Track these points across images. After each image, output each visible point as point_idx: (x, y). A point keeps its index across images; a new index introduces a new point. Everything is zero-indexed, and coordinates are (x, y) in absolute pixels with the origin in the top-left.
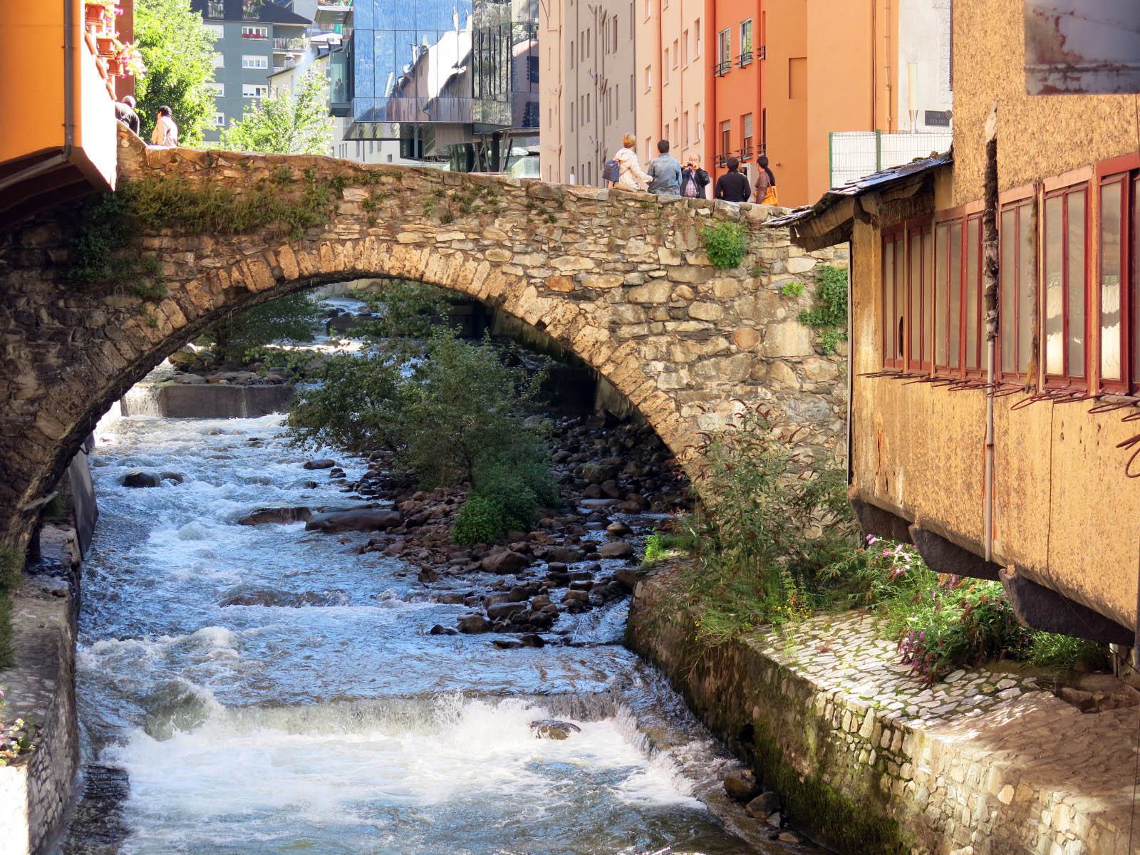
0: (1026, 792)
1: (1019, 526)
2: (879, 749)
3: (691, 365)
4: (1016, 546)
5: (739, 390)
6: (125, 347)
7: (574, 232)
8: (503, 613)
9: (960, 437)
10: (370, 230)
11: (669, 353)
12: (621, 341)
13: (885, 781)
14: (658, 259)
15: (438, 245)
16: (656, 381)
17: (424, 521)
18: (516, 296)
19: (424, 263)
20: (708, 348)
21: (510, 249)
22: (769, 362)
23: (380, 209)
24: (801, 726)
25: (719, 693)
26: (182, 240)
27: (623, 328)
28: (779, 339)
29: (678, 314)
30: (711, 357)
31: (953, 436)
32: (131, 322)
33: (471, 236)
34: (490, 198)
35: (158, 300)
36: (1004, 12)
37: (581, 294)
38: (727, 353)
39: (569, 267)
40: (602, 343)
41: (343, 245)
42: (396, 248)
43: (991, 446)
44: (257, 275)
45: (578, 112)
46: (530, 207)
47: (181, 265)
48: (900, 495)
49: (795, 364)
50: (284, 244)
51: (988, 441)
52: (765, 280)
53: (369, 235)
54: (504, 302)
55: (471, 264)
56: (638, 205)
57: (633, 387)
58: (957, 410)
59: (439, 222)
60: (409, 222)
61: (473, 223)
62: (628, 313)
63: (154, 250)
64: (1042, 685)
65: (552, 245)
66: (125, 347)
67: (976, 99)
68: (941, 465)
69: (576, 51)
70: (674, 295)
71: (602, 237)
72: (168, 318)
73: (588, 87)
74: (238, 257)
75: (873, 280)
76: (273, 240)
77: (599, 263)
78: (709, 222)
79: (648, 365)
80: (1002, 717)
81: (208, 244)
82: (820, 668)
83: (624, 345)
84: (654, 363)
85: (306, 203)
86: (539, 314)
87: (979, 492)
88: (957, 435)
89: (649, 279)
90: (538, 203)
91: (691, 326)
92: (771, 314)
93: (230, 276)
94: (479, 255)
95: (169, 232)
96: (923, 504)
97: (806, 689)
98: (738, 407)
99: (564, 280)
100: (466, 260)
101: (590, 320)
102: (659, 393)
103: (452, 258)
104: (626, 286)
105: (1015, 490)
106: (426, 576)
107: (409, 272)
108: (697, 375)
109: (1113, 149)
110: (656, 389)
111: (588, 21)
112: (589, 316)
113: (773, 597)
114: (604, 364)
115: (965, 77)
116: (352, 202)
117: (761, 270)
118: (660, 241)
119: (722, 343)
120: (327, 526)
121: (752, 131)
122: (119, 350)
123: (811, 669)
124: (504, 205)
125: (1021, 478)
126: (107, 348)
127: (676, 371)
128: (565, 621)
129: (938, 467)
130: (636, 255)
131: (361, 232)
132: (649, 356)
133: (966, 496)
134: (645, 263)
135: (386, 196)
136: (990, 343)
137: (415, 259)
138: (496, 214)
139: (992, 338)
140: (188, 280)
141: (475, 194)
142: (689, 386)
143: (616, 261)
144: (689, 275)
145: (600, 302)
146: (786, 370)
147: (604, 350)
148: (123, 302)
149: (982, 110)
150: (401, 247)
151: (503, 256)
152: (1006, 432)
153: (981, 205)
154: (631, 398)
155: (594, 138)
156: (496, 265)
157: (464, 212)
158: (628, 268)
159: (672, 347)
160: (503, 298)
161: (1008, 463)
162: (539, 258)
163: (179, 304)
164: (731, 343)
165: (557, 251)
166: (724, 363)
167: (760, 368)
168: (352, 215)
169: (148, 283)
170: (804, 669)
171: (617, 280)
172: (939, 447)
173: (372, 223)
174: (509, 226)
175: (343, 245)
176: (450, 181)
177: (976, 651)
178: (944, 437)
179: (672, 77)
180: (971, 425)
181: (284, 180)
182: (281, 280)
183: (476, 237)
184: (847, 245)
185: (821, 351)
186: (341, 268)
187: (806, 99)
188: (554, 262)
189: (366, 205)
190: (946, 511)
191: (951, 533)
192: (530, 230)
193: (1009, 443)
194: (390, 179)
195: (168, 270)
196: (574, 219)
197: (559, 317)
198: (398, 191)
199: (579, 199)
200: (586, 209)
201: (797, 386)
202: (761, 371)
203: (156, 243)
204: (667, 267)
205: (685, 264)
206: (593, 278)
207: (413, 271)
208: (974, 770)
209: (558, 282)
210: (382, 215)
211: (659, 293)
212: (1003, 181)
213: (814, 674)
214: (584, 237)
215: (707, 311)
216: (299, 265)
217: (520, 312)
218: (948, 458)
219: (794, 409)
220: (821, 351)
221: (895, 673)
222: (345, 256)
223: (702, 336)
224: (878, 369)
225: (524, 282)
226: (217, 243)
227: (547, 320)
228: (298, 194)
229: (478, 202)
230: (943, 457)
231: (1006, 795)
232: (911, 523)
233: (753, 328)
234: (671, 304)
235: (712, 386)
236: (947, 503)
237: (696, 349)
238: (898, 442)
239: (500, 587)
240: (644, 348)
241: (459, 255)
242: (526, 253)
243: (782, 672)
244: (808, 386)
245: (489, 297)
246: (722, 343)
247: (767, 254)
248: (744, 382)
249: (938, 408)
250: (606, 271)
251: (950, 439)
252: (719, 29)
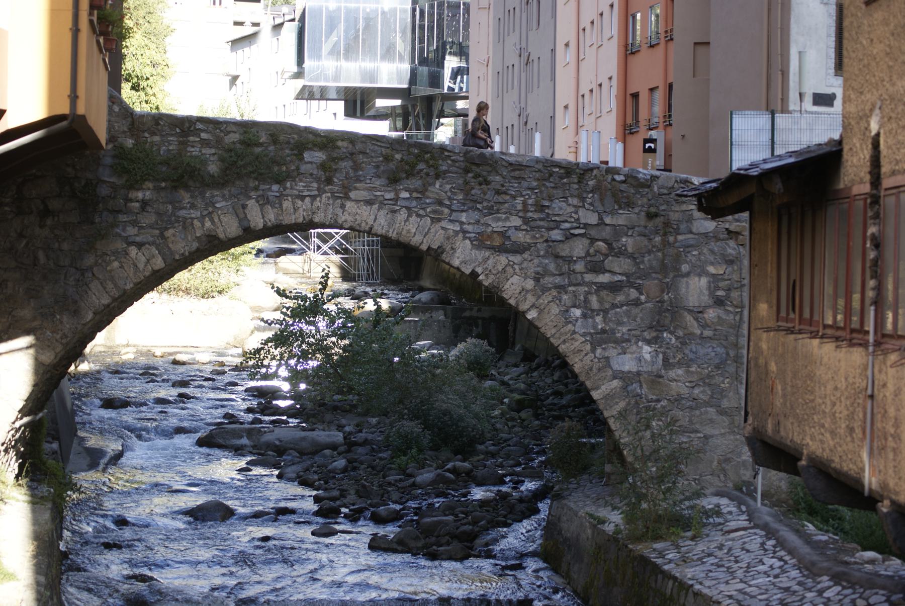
1: (895, 467)
3: (605, 312)
4: (891, 484)
5: (647, 335)
6: (110, 285)
7: (505, 193)
9: (844, 387)
10: (327, 188)
11: (586, 301)
12: (545, 290)
14: (578, 219)
15: (386, 202)
16: (574, 325)
18: (452, 248)
19: (373, 217)
20: (620, 298)
21: (449, 207)
23: (336, 170)
26: (163, 194)
27: (546, 278)
28: (683, 291)
29: (596, 268)
30: (622, 305)
31: (839, 386)
32: (116, 264)
33: (415, 195)
34: (431, 162)
36: (887, 25)
38: (637, 303)
39: (500, 224)
40: (527, 291)
41: (303, 200)
42: (349, 204)
43: (872, 397)
46: (467, 171)
49: (697, 313)
50: (250, 198)
51: (869, 392)
52: (671, 239)
53: (325, 192)
54: (442, 253)
55: (414, 219)
56: (562, 171)
57: (553, 331)
58: (843, 364)
59: (387, 181)
60: (361, 181)
61: (416, 183)
63: (138, 201)
65: (485, 204)
66: (110, 285)
67: (863, 97)
68: (827, 411)
70: (592, 251)
71: (530, 198)
72: (148, 260)
73: (512, 58)
74: (210, 209)
75: (770, 246)
77: (526, 221)
78: (623, 187)
79: (567, 311)
82: (714, 582)
83: (547, 294)
84: (573, 310)
86: (473, 265)
87: (860, 435)
88: (842, 384)
89: (569, 237)
90: (474, 167)
91: (604, 278)
92: (678, 270)
93: (203, 225)
94: (421, 212)
95: (150, 185)
96: (811, 443)
98: (647, 351)
99: (495, 235)
100: (410, 216)
101: (517, 270)
102: (577, 336)
103: (397, 215)
105: (892, 435)
107: (360, 225)
108: (610, 320)
110: (574, 332)
112: (516, 267)
114: (529, 310)
115: (854, 77)
116: (311, 163)
122: (105, 288)
123: (708, 583)
124: (444, 168)
125: (897, 425)
127: (591, 317)
129: (824, 412)
130: (558, 215)
131: (318, 189)
132: (569, 303)
133: (849, 439)
134: (566, 221)
135: (342, 159)
136: (872, 308)
137: (365, 214)
138: (437, 176)
140: (167, 229)
142: (603, 331)
143: (541, 219)
145: (526, 255)
146: (689, 318)
147: (529, 296)
149: (868, 107)
150: (353, 203)
151: (442, 213)
152: (884, 385)
153: (866, 188)
154: (552, 340)
155: (517, 103)
156: (435, 221)
157: (410, 174)
158: (552, 225)
159: (589, 296)
161: (886, 412)
163: (157, 249)
164: (641, 294)
166: (635, 311)
168: (311, 175)
170: (701, 583)
171: (542, 236)
172: (826, 395)
173: (329, 181)
174: (448, 187)
175: (303, 200)
176: (397, 147)
178: (830, 386)
179: (590, 54)
180: (854, 378)
183: (419, 195)
184: (746, 215)
186: (300, 220)
188: (488, 219)
189: (323, 166)
190: (831, 450)
191: (835, 470)
193: (888, 394)
194: (345, 144)
197: (490, 267)
198: (352, 154)
199: (511, 164)
200: (517, 173)
201: (698, 332)
203: (140, 195)
204: (586, 226)
206: (521, 235)
207: (363, 224)
209: (490, 237)
210: (337, 175)
212: (885, 169)
213: (709, 587)
214: (514, 197)
215: (621, 267)
216: (263, 217)
217: (456, 263)
218: (834, 404)
219: (695, 353)
221: (780, 588)
222: (304, 210)
223: (614, 288)
224: (772, 324)
225: (461, 235)
226: (192, 197)
227: (479, 270)
229: (421, 166)
230: (829, 403)
232: (800, 459)
233: (660, 280)
234: (589, 259)
236: (832, 443)
238: (789, 389)
240: (565, 297)
241: (404, 212)
242: (463, 211)
244: (707, 333)
245: (429, 248)
246: (633, 293)
247: (674, 216)
248: (651, 327)
249: (825, 360)
250: (532, 228)
251: (836, 388)
252: (630, 13)
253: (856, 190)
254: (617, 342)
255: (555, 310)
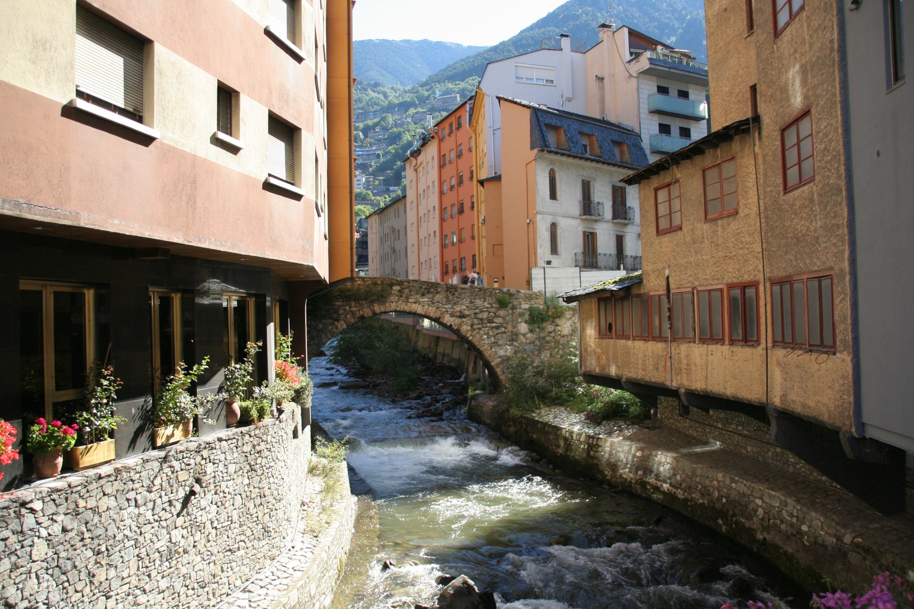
0: (647, 452)
2: (589, 444)
8: (427, 411)
13: (592, 453)
17: (378, 385)
20: (499, 331)
22: (516, 335)
24: (557, 439)
25: (516, 432)
29: (490, 321)
35: (338, 320)
37: (462, 316)
38: (505, 332)
44: (367, 312)
45: (384, 258)
47: (345, 310)
48: (613, 371)
49: (524, 335)
61: (431, 296)
62: (476, 321)
64: (633, 423)
69: (383, 239)
73: (388, 250)
76: (373, 302)
80: (628, 433)
81: (353, 304)
85: (382, 290)
89: (482, 311)
91: (494, 325)
97: (560, 429)
104: (475, 314)
106: (394, 402)
109: (735, 281)
111: (387, 230)
113: (530, 402)
117: (514, 308)
118: (485, 300)
119: (503, 329)
120: (346, 388)
121: (457, 265)
126: (323, 335)
128: (446, 414)
139: (670, 328)
141: (431, 287)
144: (493, 310)
148: (328, 321)
157: (428, 293)
160: (440, 318)
162: (450, 306)
165: (455, 304)
167: (514, 337)
169: (335, 316)
177: (612, 415)
181: (375, 284)
182: (375, 314)
185: (531, 331)
187: (502, 256)
189: (399, 291)
192: (447, 298)
195: (341, 312)
196: (460, 294)
202: (514, 337)
205: (492, 307)
208: (626, 448)
211: (485, 315)
212: (672, 286)
220: (531, 331)
223: (497, 328)
228: (379, 288)
231: (639, 454)
235: (500, 342)
237: (496, 331)
239: (418, 404)
243: (546, 424)
246: (503, 329)
247: (515, 303)
253: (651, 294)
254: (499, 346)
255: (478, 336)
